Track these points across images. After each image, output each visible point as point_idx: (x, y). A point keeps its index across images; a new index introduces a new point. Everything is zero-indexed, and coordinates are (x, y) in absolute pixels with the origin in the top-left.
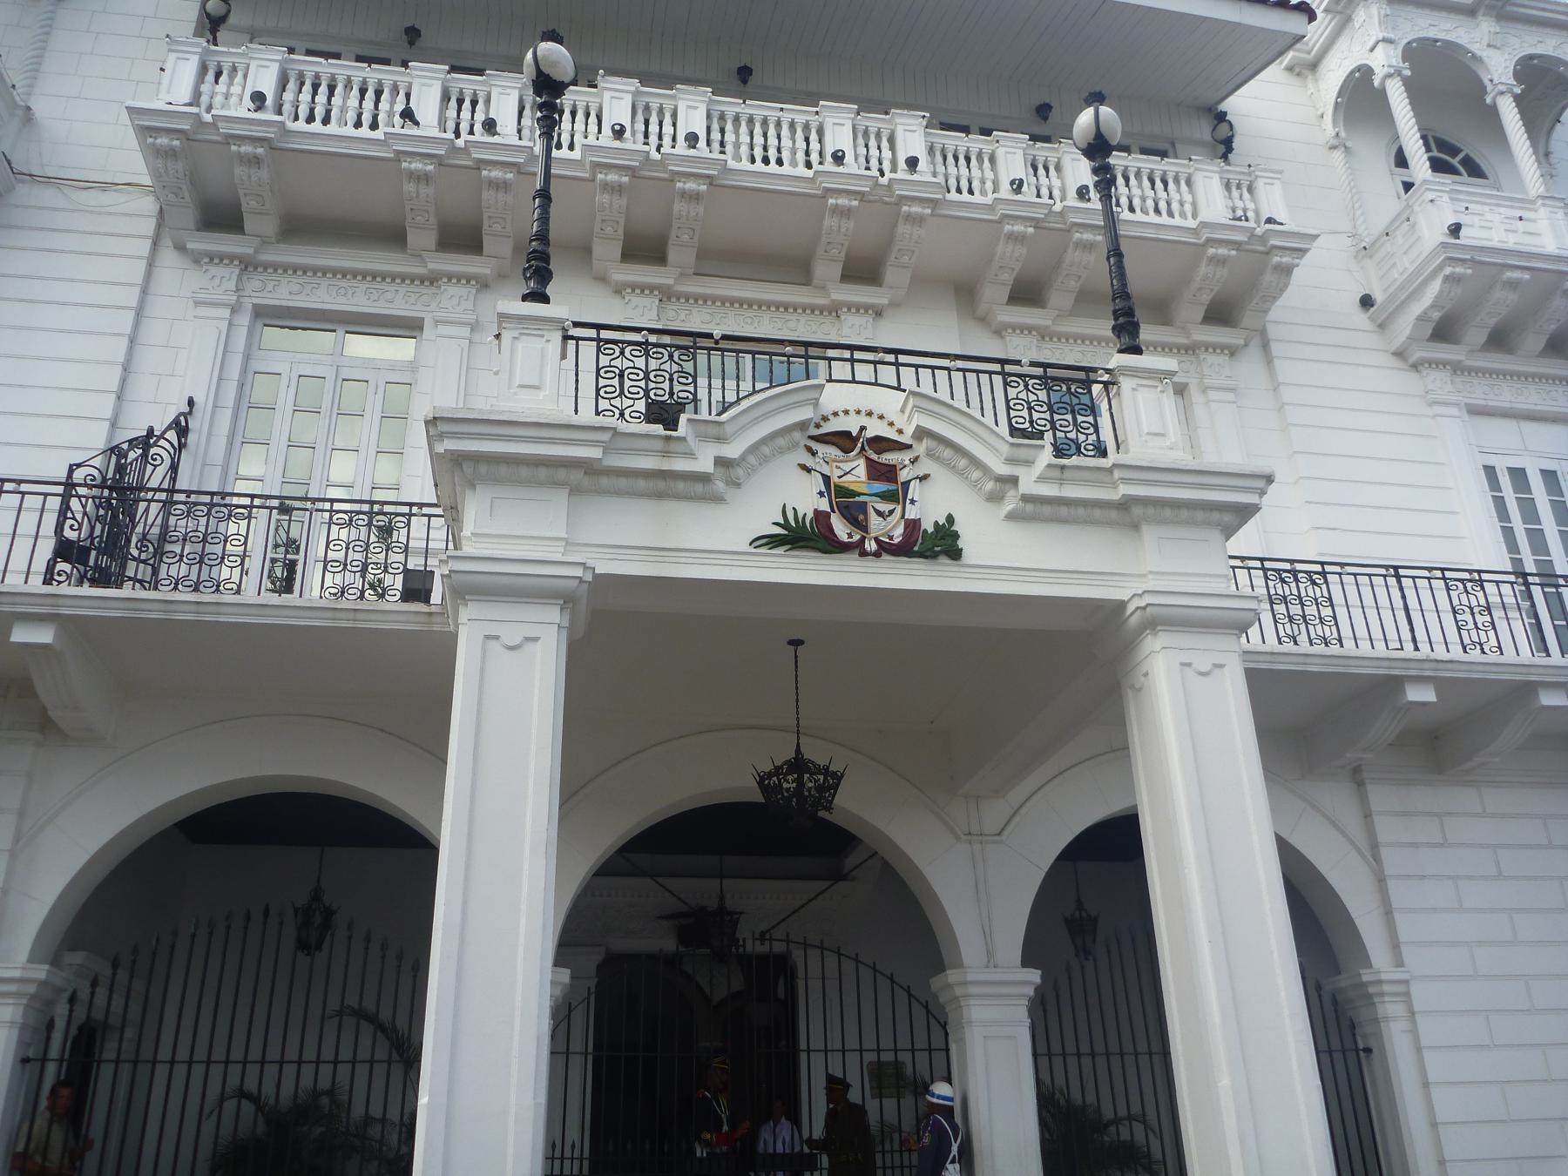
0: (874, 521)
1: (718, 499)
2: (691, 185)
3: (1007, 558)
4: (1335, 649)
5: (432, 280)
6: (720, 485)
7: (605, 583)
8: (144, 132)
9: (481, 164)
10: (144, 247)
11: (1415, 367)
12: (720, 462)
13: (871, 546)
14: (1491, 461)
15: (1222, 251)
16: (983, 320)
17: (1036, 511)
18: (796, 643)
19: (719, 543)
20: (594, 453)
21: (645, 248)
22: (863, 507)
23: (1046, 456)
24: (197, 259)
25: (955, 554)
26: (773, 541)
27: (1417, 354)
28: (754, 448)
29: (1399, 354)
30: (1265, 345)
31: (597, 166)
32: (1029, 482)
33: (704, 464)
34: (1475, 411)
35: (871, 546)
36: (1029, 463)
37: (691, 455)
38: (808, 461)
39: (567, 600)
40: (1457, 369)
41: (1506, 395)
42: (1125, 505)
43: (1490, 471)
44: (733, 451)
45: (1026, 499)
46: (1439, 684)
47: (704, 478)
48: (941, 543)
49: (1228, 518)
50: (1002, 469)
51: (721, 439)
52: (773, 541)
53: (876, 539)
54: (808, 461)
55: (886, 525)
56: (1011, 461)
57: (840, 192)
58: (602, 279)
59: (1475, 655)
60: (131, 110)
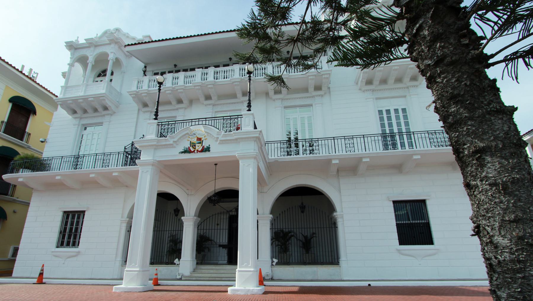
0: (197, 148)
1: (175, 147)
2: (210, 86)
3: (218, 151)
4: (318, 155)
5: (177, 109)
6: (175, 145)
7: (159, 162)
8: (130, 95)
9: (177, 90)
10: (137, 112)
11: (364, 91)
12: (174, 142)
13: (196, 151)
14: (380, 109)
15: (311, 77)
16: (271, 98)
17: (223, 142)
18: (216, 164)
19: (174, 154)
20: (155, 143)
21: (208, 97)
22: (195, 146)
23: (223, 133)
24: (144, 112)
25: (209, 151)
26: (182, 152)
27: (363, 89)
28: (180, 138)
29: (360, 89)
30: (330, 92)
31: (195, 86)
32: (221, 138)
33: (171, 142)
34: (377, 99)
35: (196, 151)
36: (220, 134)
37: (169, 141)
38: (188, 139)
39: (153, 165)
40: (373, 90)
41: (387, 94)
42: (236, 139)
43: (380, 112)
44: (175, 140)
45: (221, 140)
46: (340, 159)
47: (172, 144)
48: (208, 149)
49: (255, 139)
50: (216, 136)
51: (174, 138)
52: (182, 152)
53: (197, 150)
54: (188, 139)
55: (199, 147)
56: (218, 135)
57: (235, 82)
58: (203, 104)
59: (349, 153)
60: (128, 92)
